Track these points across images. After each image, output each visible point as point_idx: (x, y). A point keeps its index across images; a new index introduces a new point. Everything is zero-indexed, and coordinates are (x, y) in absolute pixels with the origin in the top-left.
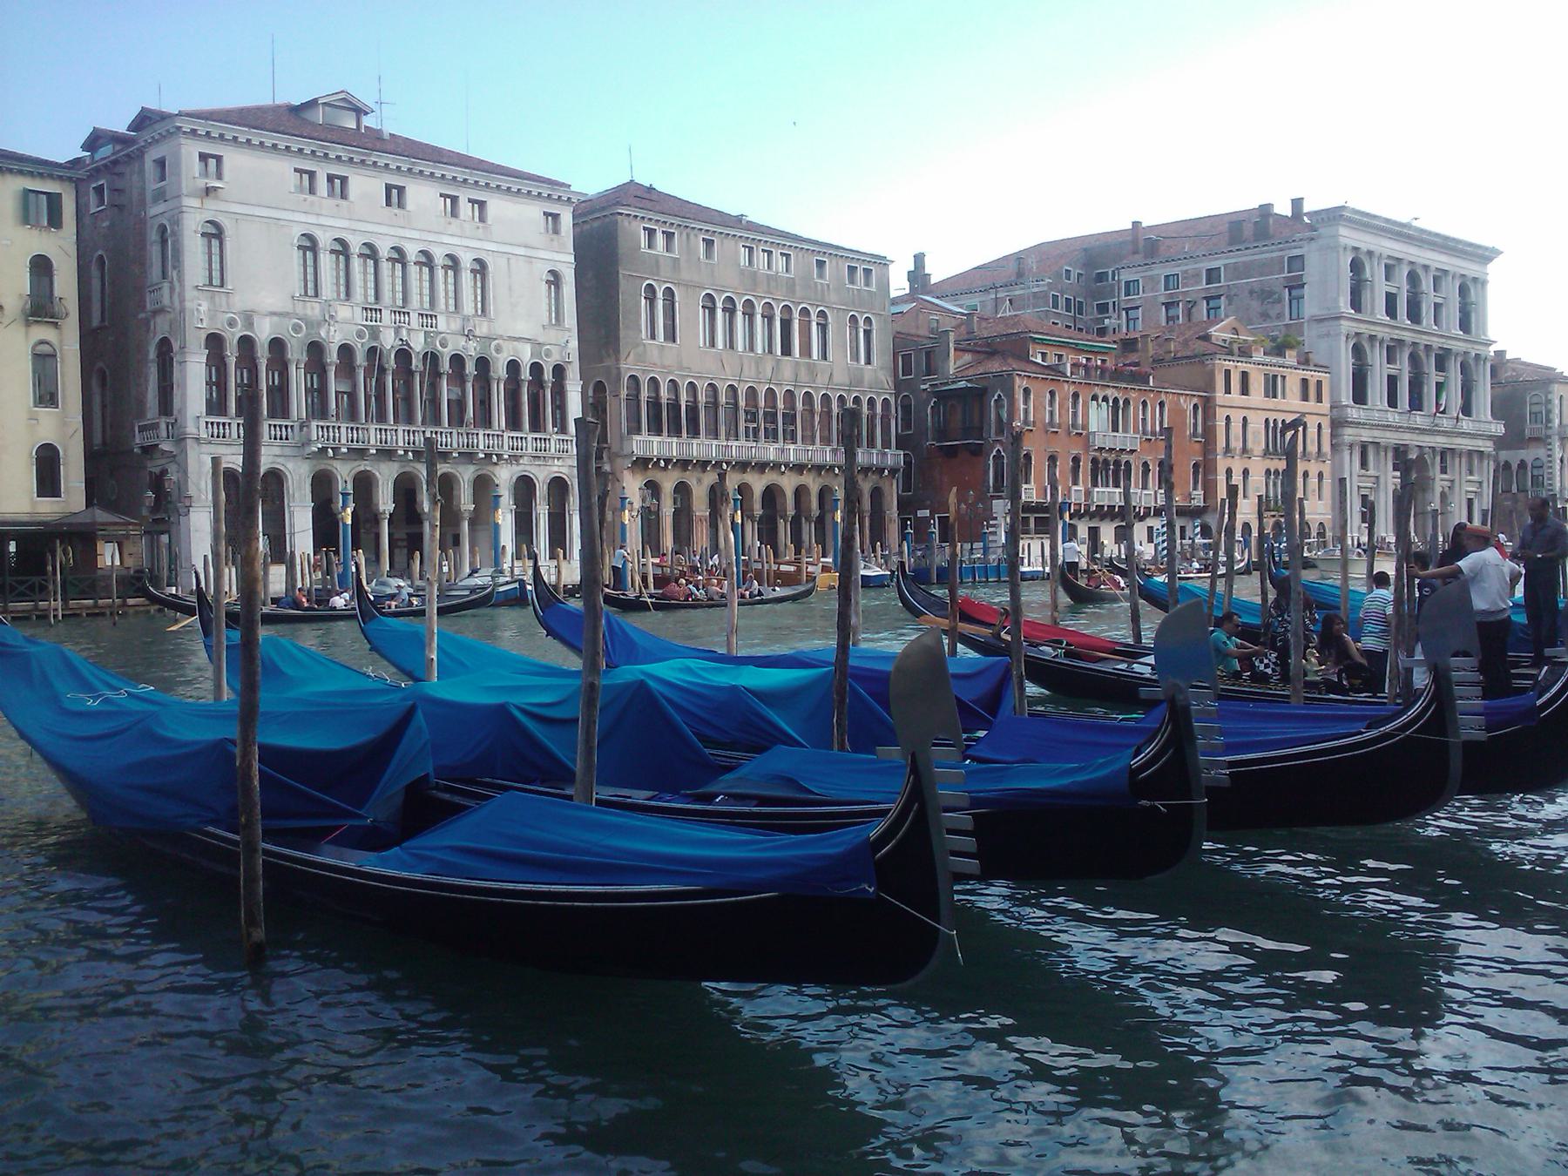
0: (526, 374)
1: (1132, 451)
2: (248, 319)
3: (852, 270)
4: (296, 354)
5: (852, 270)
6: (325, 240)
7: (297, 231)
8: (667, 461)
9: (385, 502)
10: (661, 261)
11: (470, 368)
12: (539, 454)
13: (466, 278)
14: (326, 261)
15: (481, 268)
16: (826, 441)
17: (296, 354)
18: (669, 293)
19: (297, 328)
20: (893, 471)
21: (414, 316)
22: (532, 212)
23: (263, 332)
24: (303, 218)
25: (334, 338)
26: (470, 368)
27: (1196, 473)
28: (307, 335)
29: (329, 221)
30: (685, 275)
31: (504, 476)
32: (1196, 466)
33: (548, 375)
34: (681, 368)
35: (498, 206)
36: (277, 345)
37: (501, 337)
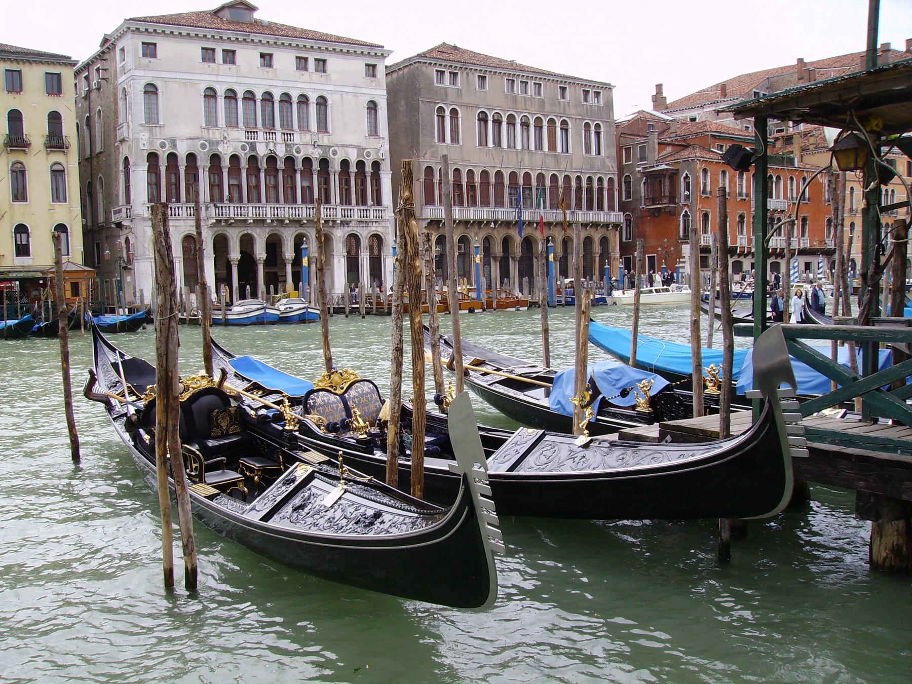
0: (353, 169)
1: (782, 211)
3: (586, 93)
4: (203, 163)
5: (586, 93)
6: (221, 91)
7: (203, 87)
8: (495, 222)
9: (260, 252)
10: (449, 90)
11: (316, 166)
12: (362, 219)
14: (221, 102)
15: (322, 102)
17: (203, 163)
18: (454, 112)
19: (203, 146)
20: (616, 226)
22: (358, 65)
23: (182, 151)
24: (207, 78)
25: (226, 152)
26: (316, 166)
27: (829, 224)
28: (209, 151)
29: (223, 77)
30: (465, 99)
31: (339, 235)
32: (829, 221)
33: (368, 169)
34: (464, 161)
35: (334, 63)
36: (191, 157)
37: (337, 145)
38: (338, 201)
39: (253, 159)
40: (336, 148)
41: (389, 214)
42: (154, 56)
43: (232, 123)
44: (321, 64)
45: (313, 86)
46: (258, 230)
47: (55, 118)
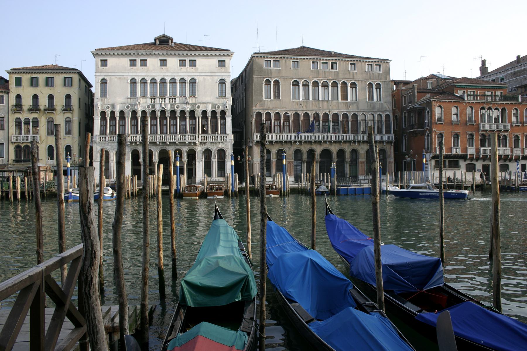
2: (113, 106)
6: (138, 80)
13: (188, 85)
14: (138, 85)
15: (193, 82)
16: (388, 132)
18: (277, 82)
21: (168, 100)
24: (131, 74)
25: (139, 109)
29: (139, 73)
30: (284, 74)
31: (199, 149)
33: (218, 115)
35: (200, 61)
37: (200, 103)
38: (200, 132)
39: (154, 113)
41: (231, 137)
42: (106, 65)
43: (144, 95)
44: (193, 63)
45: (187, 74)
46: (154, 147)
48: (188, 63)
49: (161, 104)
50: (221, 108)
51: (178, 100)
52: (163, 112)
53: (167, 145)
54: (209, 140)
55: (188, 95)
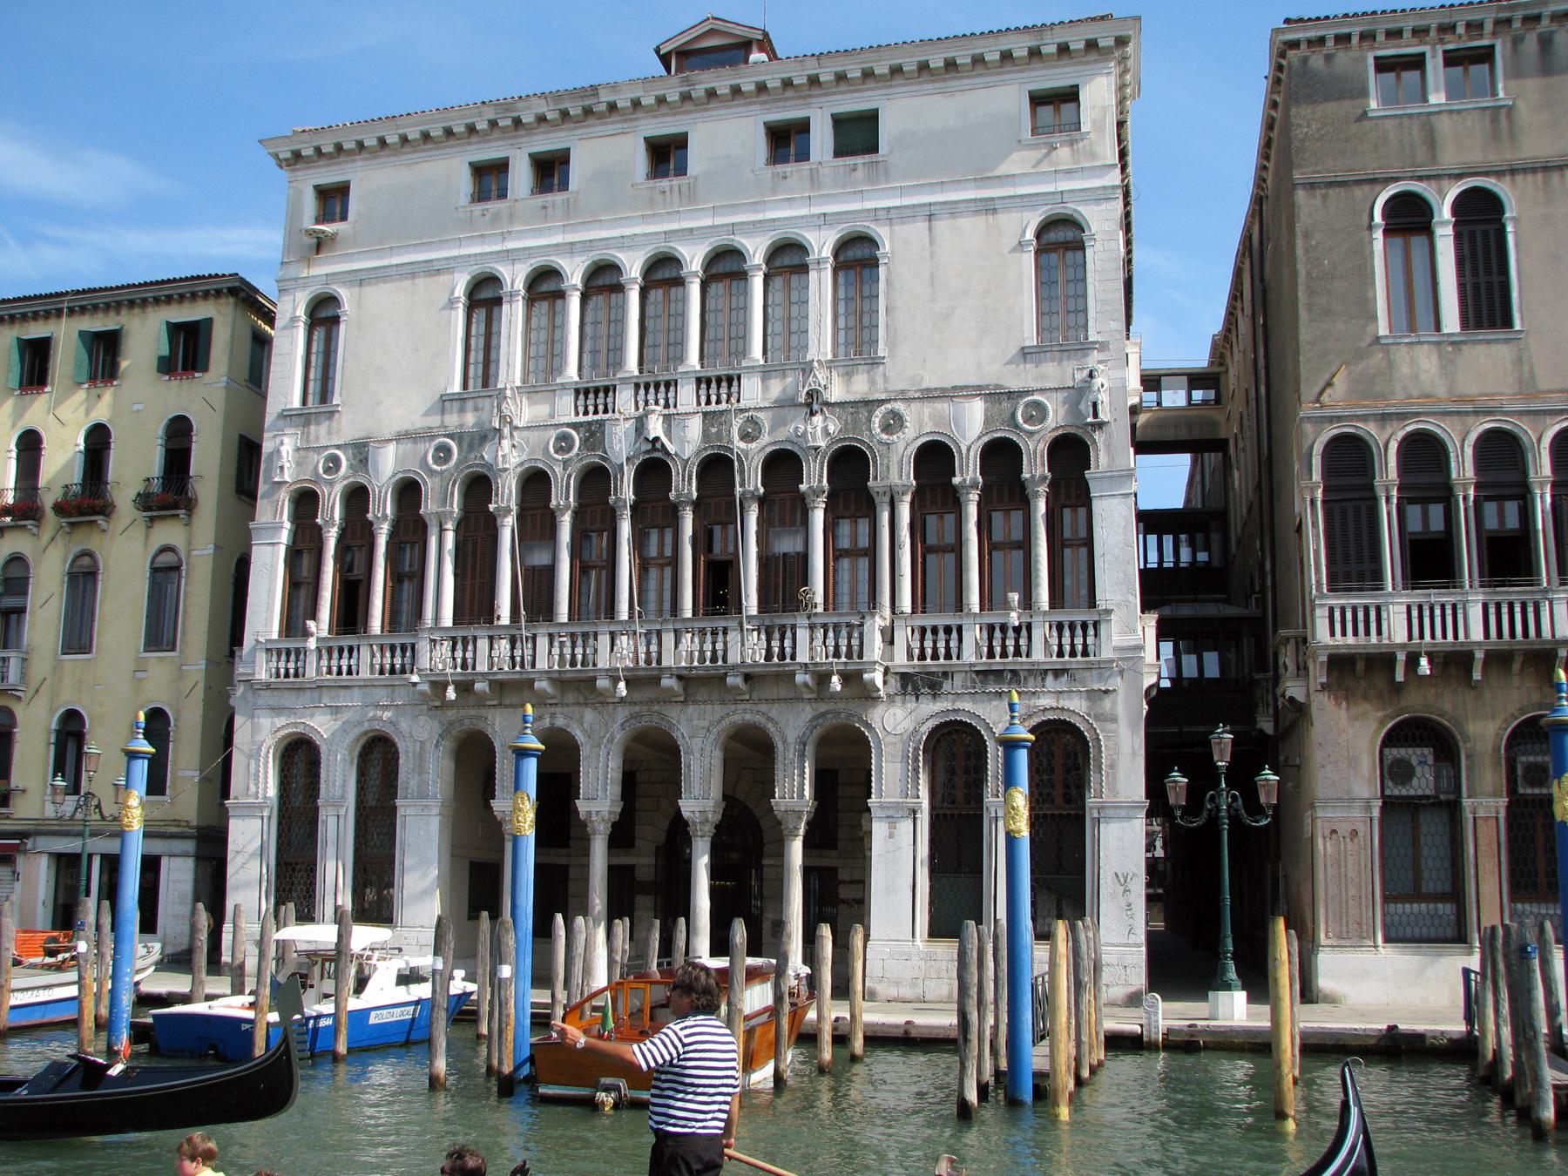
2: (361, 452)
13: (821, 285)
14: (513, 315)
15: (857, 258)
17: (442, 505)
18: (1480, 213)
19: (443, 453)
25: (509, 460)
29: (522, 239)
30: (1536, 146)
31: (896, 726)
33: (1035, 467)
36: (408, 491)
38: (906, 603)
39: (595, 479)
40: (899, 406)
46: (589, 715)
47: (179, 433)
48: (821, 138)
49: (641, 424)
50: (1056, 418)
51: (753, 392)
52: (654, 469)
53: (668, 698)
54: (969, 656)
55: (821, 340)
